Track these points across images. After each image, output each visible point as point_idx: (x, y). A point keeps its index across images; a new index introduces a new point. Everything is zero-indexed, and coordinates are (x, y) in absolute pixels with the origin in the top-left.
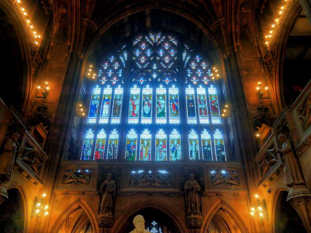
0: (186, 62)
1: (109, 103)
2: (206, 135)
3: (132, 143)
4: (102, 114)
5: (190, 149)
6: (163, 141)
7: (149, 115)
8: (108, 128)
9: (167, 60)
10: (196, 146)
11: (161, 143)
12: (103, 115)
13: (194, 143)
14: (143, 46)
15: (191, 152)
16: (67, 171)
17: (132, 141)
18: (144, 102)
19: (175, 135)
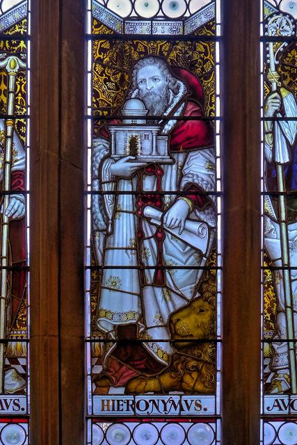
11: (152, 78)
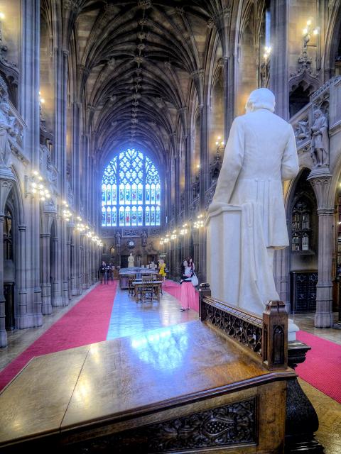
2: (153, 209)
8: (112, 206)
14: (125, 160)
19: (140, 209)
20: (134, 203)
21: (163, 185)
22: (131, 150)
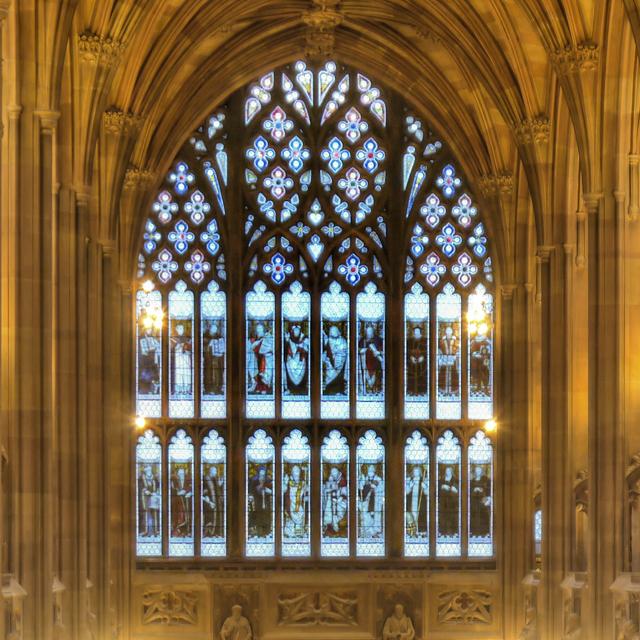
0: (413, 194)
1: (189, 349)
3: (262, 473)
4: (173, 384)
5: (406, 491)
6: (341, 467)
7: (297, 390)
8: (197, 429)
9: (353, 185)
10: (421, 481)
11: (335, 472)
12: (177, 389)
13: (417, 472)
14: (278, 125)
15: (410, 497)
16: (146, 596)
17: (261, 466)
18: (287, 346)
19: (371, 448)
20: (334, 409)
21: (510, 308)
22: (315, 66)
